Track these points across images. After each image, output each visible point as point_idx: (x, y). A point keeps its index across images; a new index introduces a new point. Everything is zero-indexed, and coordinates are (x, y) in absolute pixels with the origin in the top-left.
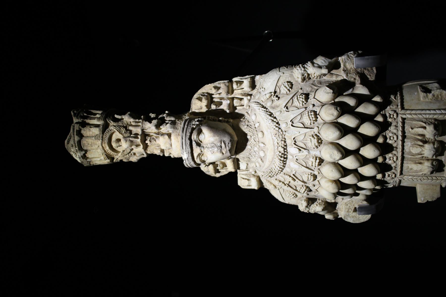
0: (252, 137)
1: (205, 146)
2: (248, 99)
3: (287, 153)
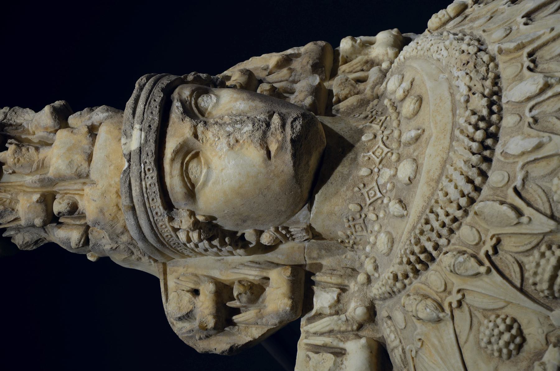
0: (379, 137)
1: (212, 121)
2: (381, 70)
3: (501, 119)
